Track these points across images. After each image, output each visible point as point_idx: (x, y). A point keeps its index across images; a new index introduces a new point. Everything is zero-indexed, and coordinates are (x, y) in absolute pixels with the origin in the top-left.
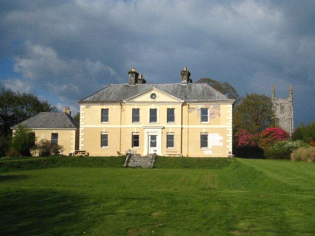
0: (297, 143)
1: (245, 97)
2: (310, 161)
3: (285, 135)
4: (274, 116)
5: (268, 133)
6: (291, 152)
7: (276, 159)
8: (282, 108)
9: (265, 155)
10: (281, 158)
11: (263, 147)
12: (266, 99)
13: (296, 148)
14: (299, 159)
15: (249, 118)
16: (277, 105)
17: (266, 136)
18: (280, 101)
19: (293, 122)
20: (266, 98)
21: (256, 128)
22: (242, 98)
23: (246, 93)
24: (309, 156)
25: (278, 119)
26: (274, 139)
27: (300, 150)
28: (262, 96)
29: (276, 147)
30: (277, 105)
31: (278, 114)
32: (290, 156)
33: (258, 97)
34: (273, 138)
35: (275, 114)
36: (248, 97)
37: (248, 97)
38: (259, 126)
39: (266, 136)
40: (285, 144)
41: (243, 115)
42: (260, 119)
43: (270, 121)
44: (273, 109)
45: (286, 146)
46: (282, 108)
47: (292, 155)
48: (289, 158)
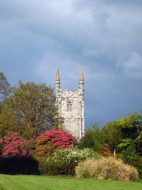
0: (86, 151)
1: (18, 87)
2: (101, 178)
3: (70, 141)
4: (57, 114)
5: (47, 138)
6: (76, 164)
7: (55, 174)
8: (69, 103)
9: (40, 169)
10: (63, 173)
11: (38, 159)
12: (48, 90)
13: (83, 159)
14: (86, 175)
15: (22, 117)
16: (63, 99)
17: (45, 143)
18: (66, 94)
19: (83, 124)
20: (47, 89)
21: (32, 130)
22: (13, 88)
23: (20, 82)
24: (100, 170)
25: (62, 118)
26: (56, 147)
27: (89, 161)
28: (42, 87)
29: (55, 158)
30: (63, 99)
31: (63, 111)
32: (74, 171)
33: (35, 86)
34: (55, 145)
35: (59, 111)
36: (22, 86)
37: (22, 86)
38: (36, 128)
39: (45, 143)
40: (68, 153)
41: (15, 112)
42: (37, 119)
43: (52, 122)
44: (56, 105)
45: (69, 156)
46: (69, 103)
47: (78, 169)
48: (73, 174)
